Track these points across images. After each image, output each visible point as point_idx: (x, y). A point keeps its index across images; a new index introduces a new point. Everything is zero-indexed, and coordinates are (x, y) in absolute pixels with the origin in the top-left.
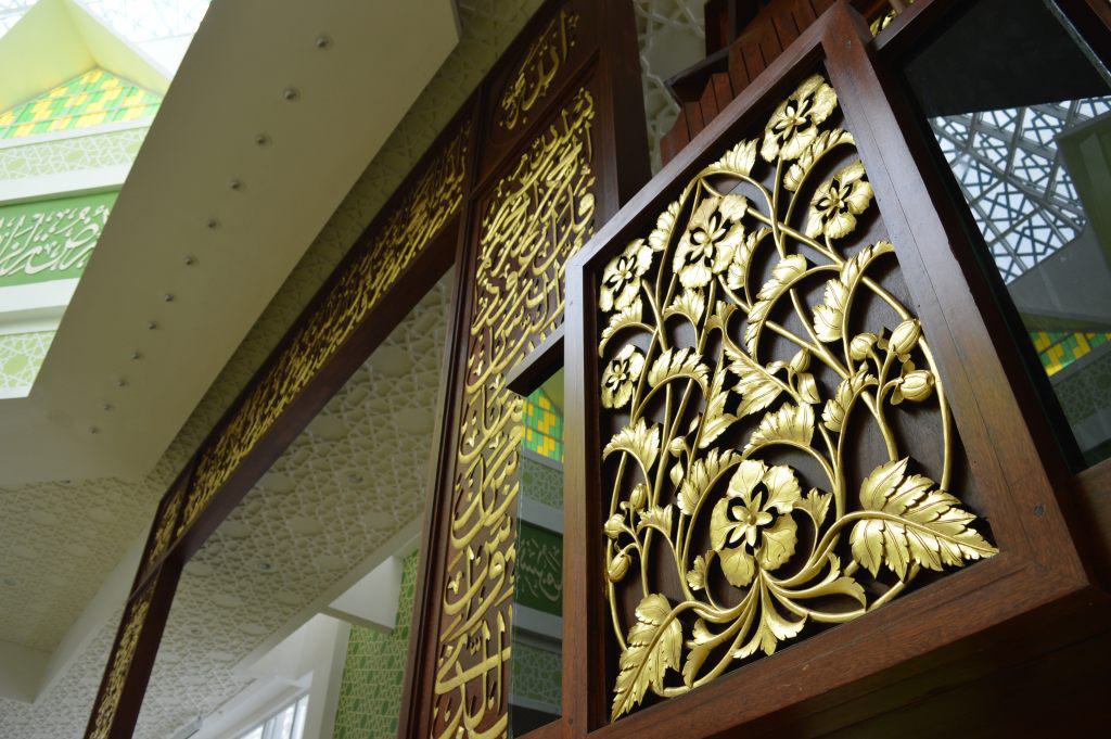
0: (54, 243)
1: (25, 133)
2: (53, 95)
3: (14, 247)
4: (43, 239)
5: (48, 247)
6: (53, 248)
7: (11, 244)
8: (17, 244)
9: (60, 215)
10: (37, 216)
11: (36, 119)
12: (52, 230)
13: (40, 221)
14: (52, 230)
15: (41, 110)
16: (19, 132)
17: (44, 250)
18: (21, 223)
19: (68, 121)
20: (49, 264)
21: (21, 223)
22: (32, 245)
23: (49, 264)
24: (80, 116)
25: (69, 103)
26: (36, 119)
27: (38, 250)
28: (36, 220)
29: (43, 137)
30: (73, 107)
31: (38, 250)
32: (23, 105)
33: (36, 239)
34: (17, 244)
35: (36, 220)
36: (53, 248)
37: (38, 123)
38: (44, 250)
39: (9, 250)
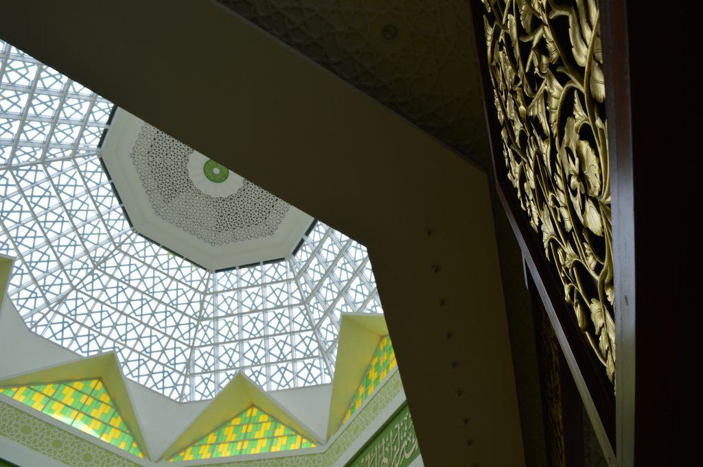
0: (411, 435)
1: (372, 390)
2: (374, 364)
3: (395, 449)
4: (405, 436)
5: (409, 439)
6: (411, 438)
7: (393, 448)
8: (395, 447)
9: (405, 418)
10: (396, 427)
11: (373, 381)
12: (406, 429)
13: (399, 428)
14: (406, 429)
15: (373, 375)
16: (369, 393)
17: (408, 441)
18: (391, 435)
19: (385, 372)
20: (413, 448)
21: (391, 435)
22: (402, 442)
23: (413, 449)
24: (389, 365)
25: (381, 364)
26: (373, 381)
27: (405, 443)
28: (397, 429)
29: (379, 386)
30: (384, 363)
31: (405, 443)
32: (364, 379)
33: (402, 438)
34: (395, 447)
35: (397, 429)
36: (411, 438)
37: (374, 382)
38: (408, 441)
39: (394, 453)
